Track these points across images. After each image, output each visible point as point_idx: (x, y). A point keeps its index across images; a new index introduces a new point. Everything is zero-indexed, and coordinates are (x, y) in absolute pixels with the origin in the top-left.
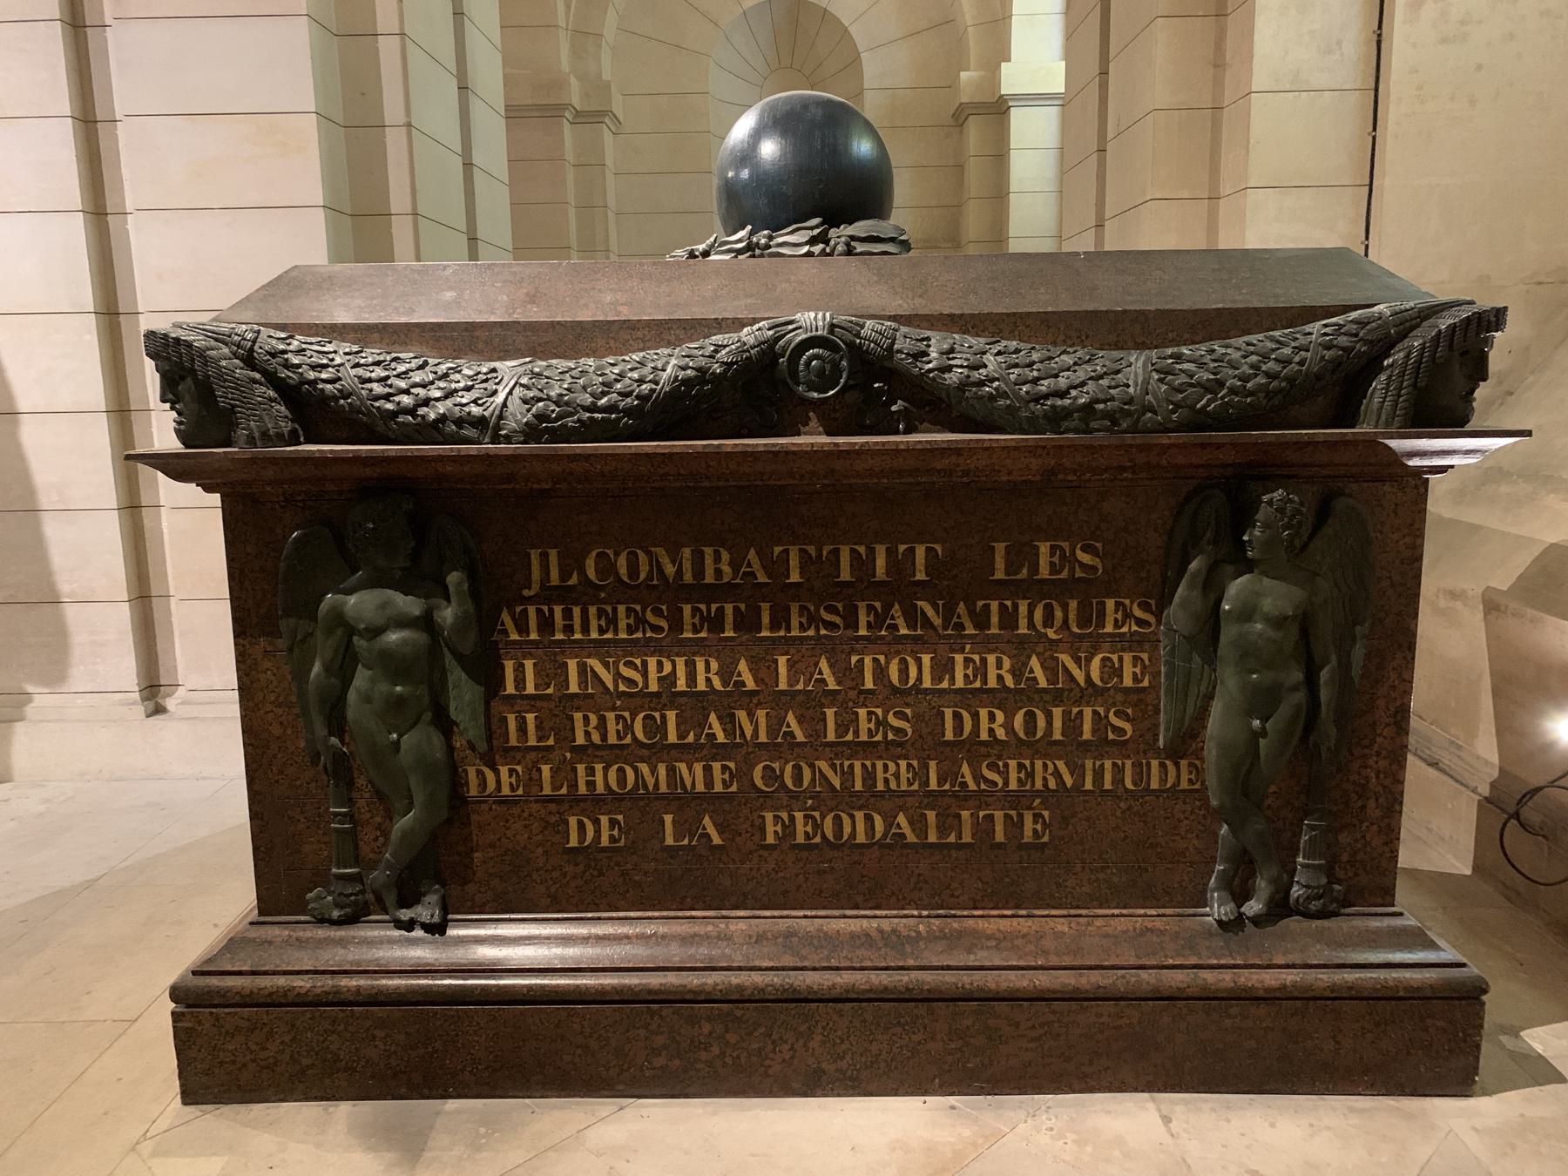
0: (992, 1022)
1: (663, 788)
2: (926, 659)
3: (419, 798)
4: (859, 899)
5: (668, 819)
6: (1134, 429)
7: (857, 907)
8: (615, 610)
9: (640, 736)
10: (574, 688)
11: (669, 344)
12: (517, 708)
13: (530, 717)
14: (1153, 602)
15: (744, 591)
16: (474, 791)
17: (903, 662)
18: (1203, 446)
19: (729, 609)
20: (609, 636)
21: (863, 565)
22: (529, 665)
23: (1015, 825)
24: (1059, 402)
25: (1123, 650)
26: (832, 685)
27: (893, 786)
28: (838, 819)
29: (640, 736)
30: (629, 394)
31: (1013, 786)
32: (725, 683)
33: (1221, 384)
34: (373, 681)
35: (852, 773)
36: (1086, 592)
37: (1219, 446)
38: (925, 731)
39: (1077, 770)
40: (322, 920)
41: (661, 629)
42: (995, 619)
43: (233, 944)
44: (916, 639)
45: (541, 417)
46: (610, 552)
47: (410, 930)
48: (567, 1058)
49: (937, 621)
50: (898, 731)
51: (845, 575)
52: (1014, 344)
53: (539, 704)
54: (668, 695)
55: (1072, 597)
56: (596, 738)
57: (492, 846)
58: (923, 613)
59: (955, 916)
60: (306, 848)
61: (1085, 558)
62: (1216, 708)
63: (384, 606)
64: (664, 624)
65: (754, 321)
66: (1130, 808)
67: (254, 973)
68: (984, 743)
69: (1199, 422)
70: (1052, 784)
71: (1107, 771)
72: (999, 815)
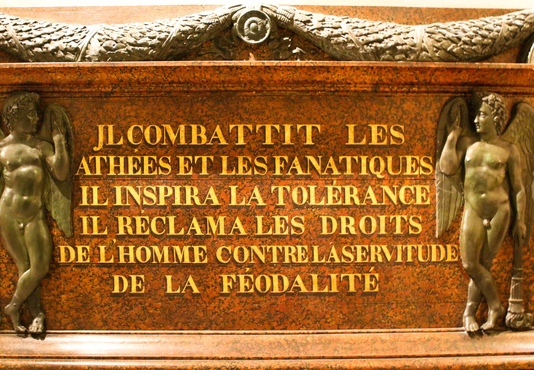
1: (166, 261)
2: (312, 188)
3: (33, 260)
4: (275, 324)
6: (417, 60)
7: (273, 329)
8: (142, 159)
10: (119, 202)
12: (88, 213)
13: (95, 219)
14: (430, 158)
15: (212, 149)
16: (63, 260)
17: (300, 190)
19: (204, 159)
20: (139, 173)
21: (278, 135)
22: (95, 189)
23: (360, 282)
24: (379, 45)
25: (416, 184)
26: (261, 203)
27: (294, 260)
28: (263, 280)
30: (153, 38)
32: (202, 201)
33: (459, 39)
34: (12, 194)
35: (271, 253)
36: (396, 150)
37: (460, 70)
38: (312, 229)
41: (167, 170)
42: (349, 166)
44: (308, 178)
46: (141, 127)
49: (318, 168)
50: (297, 229)
51: (269, 141)
53: (100, 211)
54: (170, 208)
55: (389, 155)
56: (130, 231)
57: (72, 291)
59: (327, 333)
62: (466, 214)
63: (20, 152)
64: (168, 167)
66: (421, 272)
68: (344, 236)
69: (451, 57)
70: (380, 259)
71: (407, 251)
72: (352, 277)
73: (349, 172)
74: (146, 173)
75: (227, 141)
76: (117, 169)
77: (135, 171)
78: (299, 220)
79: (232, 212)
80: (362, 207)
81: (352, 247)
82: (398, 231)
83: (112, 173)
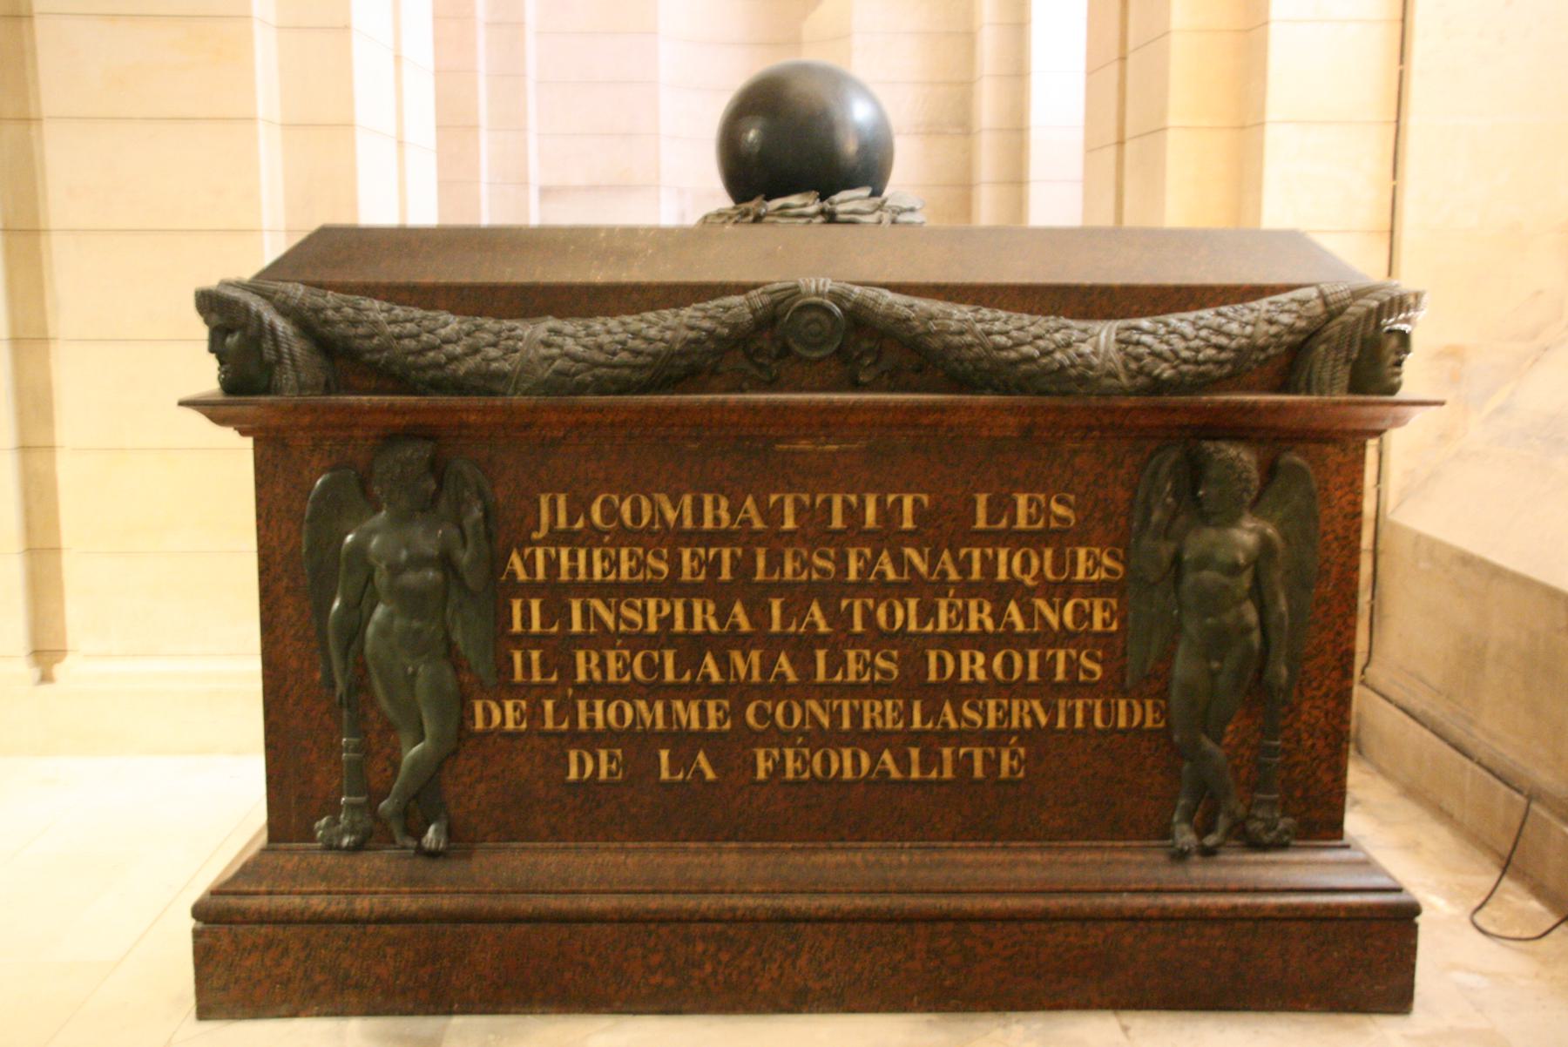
1: (660, 725)
3: (429, 729)
5: (664, 755)
7: (842, 840)
8: (618, 555)
13: (535, 655)
15: (742, 537)
21: (854, 514)
23: (992, 763)
26: (823, 628)
27: (879, 724)
28: (826, 760)
31: (991, 724)
32: (721, 624)
33: (1175, 353)
34: (390, 616)
37: (1174, 410)
39: (1051, 710)
42: (976, 566)
44: (904, 585)
45: (558, 373)
46: (615, 498)
48: (568, 975)
49: (923, 568)
50: (886, 673)
51: (837, 522)
54: (665, 636)
55: (1047, 545)
56: (597, 675)
58: (910, 562)
60: (317, 778)
64: (664, 567)
66: (1099, 746)
67: (270, 893)
68: (965, 684)
69: (1157, 386)
70: (1028, 723)
71: (1077, 712)
72: (978, 753)
75: (766, 523)
76: (574, 571)
77: (604, 574)
78: (887, 657)
80: (996, 635)
81: (980, 704)
82: (1060, 676)
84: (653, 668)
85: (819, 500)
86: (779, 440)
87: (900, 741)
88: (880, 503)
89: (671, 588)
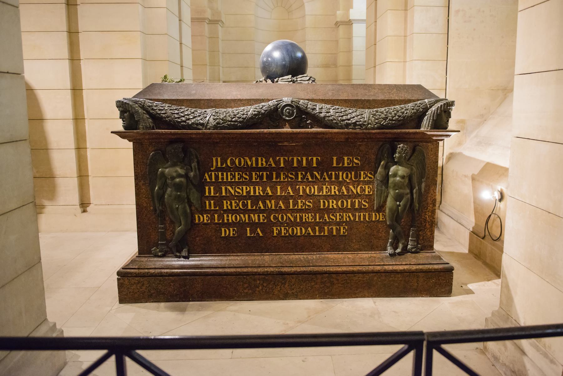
0: (332, 280)
1: (247, 221)
2: (316, 187)
3: (183, 223)
5: (248, 229)
6: (366, 129)
9: (241, 207)
10: (224, 194)
11: (250, 105)
13: (212, 202)
16: (197, 221)
17: (310, 187)
18: (383, 133)
19: (265, 173)
20: (233, 180)
21: (300, 162)
22: (212, 188)
23: (338, 231)
24: (348, 122)
26: (292, 194)
27: (307, 220)
28: (293, 229)
29: (241, 207)
31: (338, 220)
32: (264, 193)
34: (171, 191)
36: (356, 169)
37: (387, 133)
39: (354, 216)
40: (156, 256)
42: (333, 177)
43: (133, 261)
44: (313, 182)
45: (218, 123)
47: (180, 258)
49: (319, 177)
50: (309, 206)
51: (295, 165)
52: (337, 107)
54: (248, 196)
56: (229, 207)
58: (315, 175)
60: (152, 237)
61: (356, 161)
62: (389, 200)
64: (247, 177)
65: (272, 100)
67: (138, 269)
68: (331, 209)
69: (382, 127)
70: (348, 219)
72: (334, 228)
73: (333, 179)
74: (237, 180)
76: (223, 179)
77: (231, 179)
79: (278, 198)
80: (339, 195)
82: (357, 206)
83: (220, 180)
84: (245, 205)
85: (290, 158)
86: (280, 142)
87: (313, 225)
88: (307, 159)
89: (250, 183)
